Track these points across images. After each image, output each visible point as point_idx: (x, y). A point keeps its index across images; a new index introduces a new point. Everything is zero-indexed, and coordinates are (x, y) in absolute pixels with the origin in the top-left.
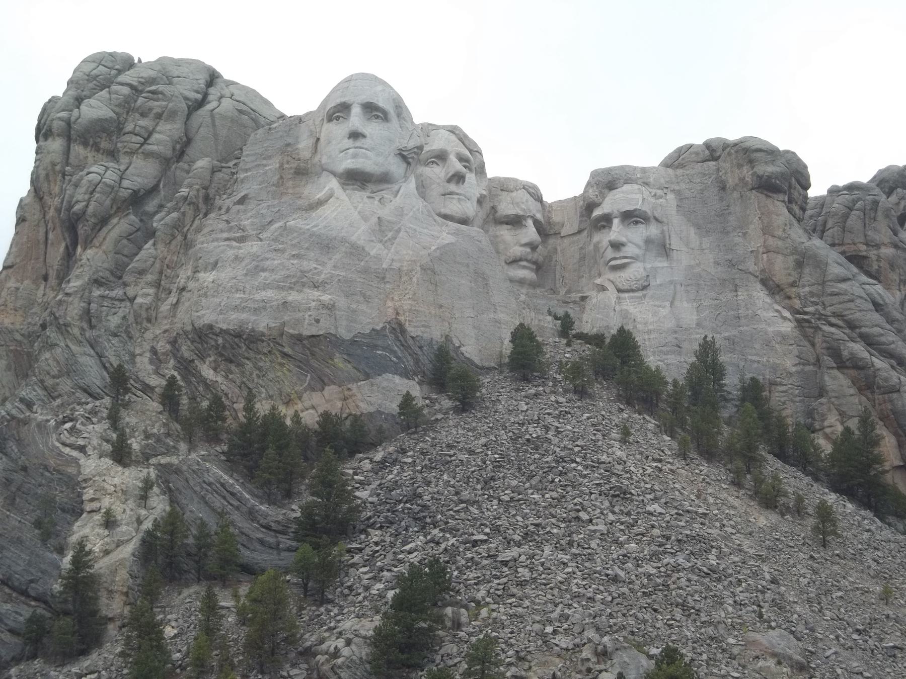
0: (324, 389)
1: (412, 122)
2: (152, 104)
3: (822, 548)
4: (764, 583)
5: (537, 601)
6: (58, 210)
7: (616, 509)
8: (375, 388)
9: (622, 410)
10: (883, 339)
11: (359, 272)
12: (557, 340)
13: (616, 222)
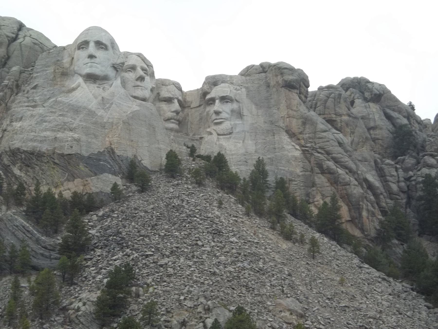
0: (74, 180)
1: (119, 51)
3: (312, 259)
4: (285, 276)
5: (177, 284)
7: (215, 240)
8: (99, 180)
9: (219, 192)
10: (342, 160)
11: (92, 123)
12: (188, 158)
13: (217, 101)
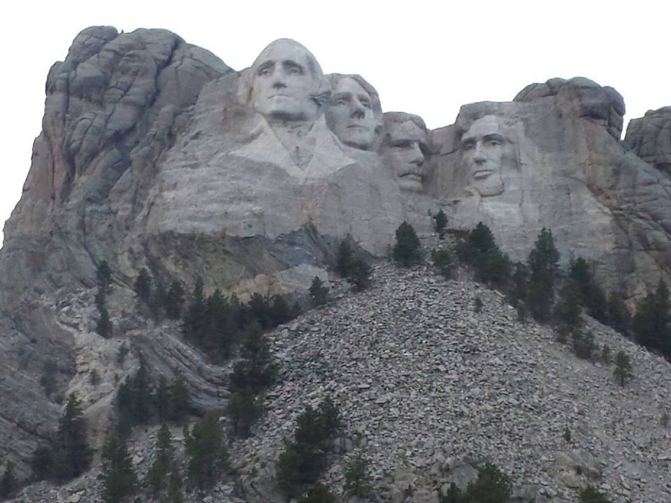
0: (254, 277)
2: (130, 64)
4: (573, 415)
5: (403, 432)
6: (61, 147)
7: (467, 362)
12: (433, 234)
13: (479, 144)
